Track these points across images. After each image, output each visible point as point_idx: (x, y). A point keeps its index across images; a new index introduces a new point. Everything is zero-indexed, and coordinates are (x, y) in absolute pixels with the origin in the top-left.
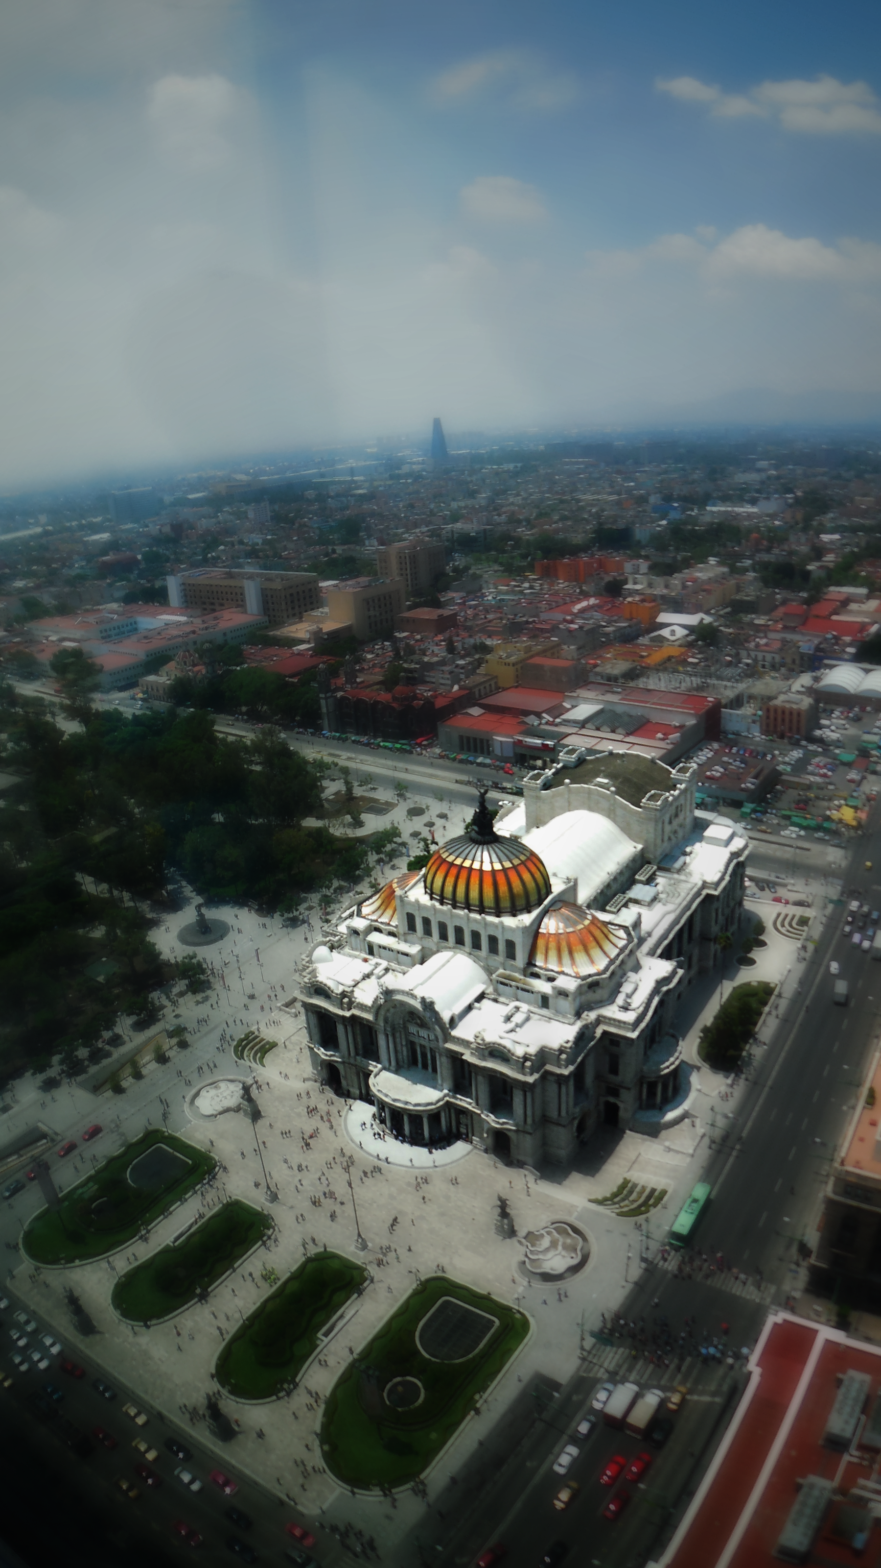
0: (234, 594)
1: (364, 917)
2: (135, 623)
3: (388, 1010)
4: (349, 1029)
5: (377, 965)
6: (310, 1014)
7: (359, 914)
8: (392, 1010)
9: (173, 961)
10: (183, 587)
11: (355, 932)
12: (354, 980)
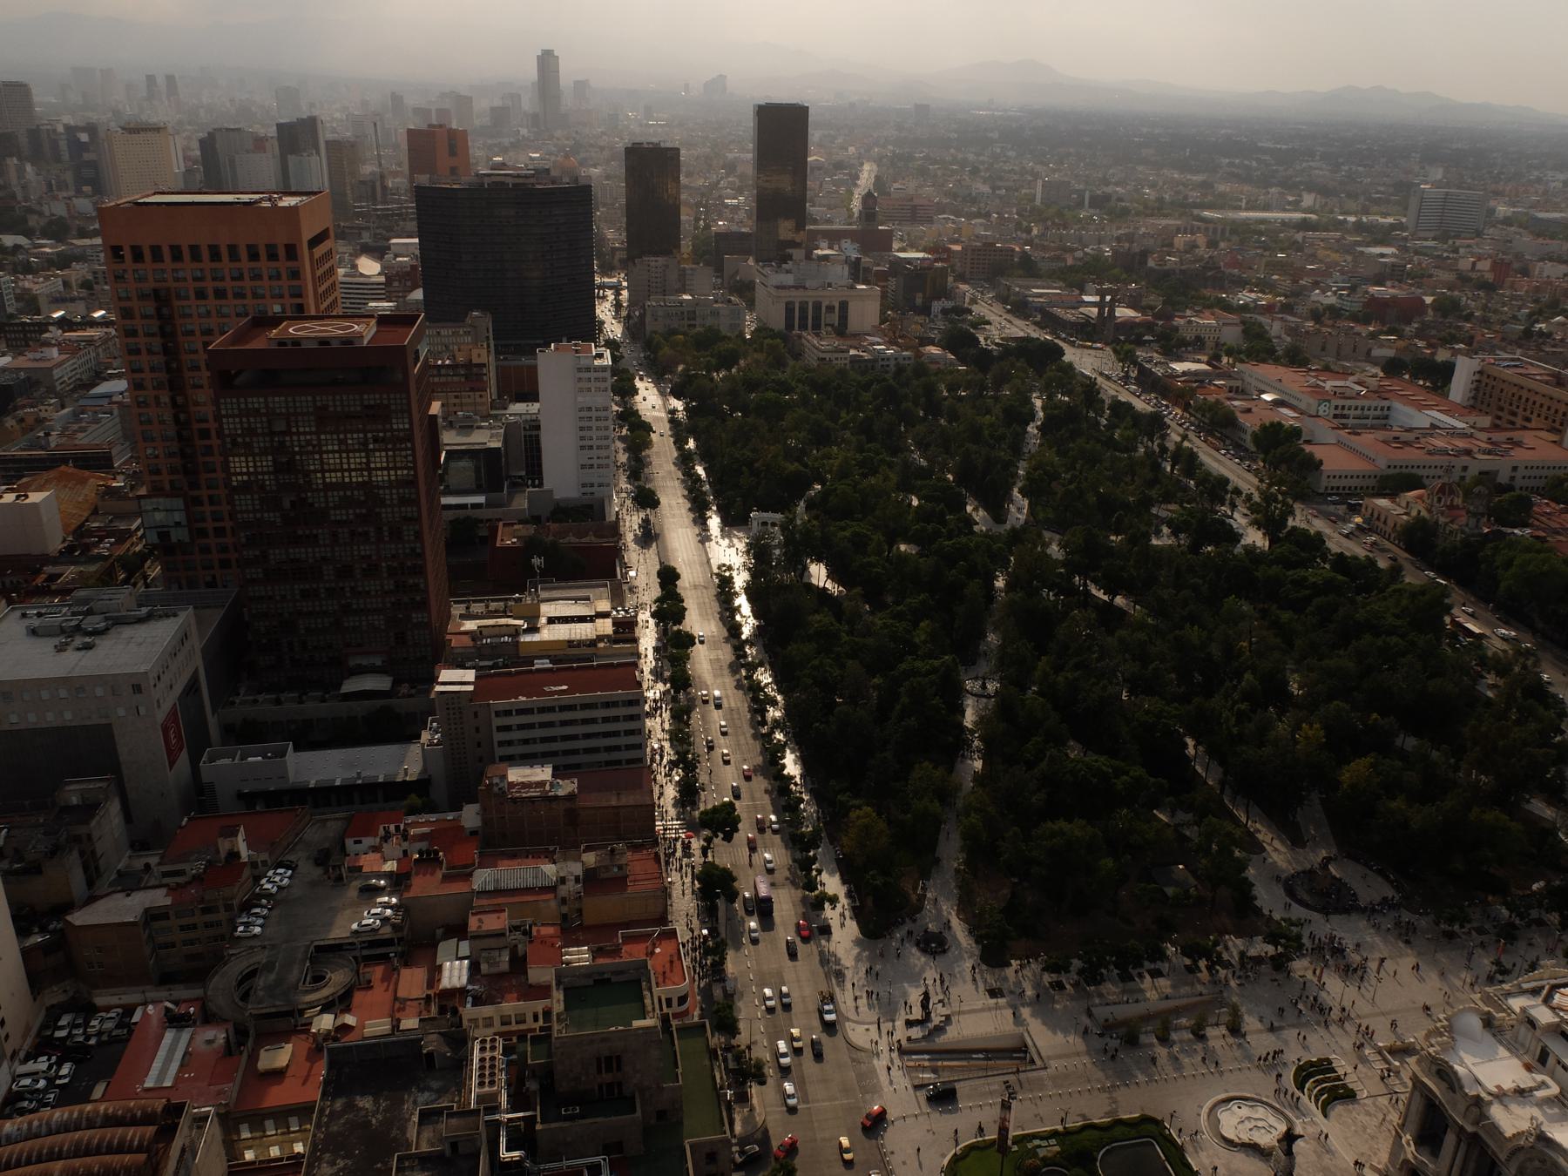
0: (1553, 411)
1: (1553, 1009)
2: (1389, 408)
3: (1531, 1160)
4: (1463, 1146)
5: (1543, 1085)
6: (1417, 1094)
7: (1547, 1001)
8: (1537, 1163)
9: (1266, 912)
10: (1477, 377)
11: (1531, 1023)
12: (1498, 1087)
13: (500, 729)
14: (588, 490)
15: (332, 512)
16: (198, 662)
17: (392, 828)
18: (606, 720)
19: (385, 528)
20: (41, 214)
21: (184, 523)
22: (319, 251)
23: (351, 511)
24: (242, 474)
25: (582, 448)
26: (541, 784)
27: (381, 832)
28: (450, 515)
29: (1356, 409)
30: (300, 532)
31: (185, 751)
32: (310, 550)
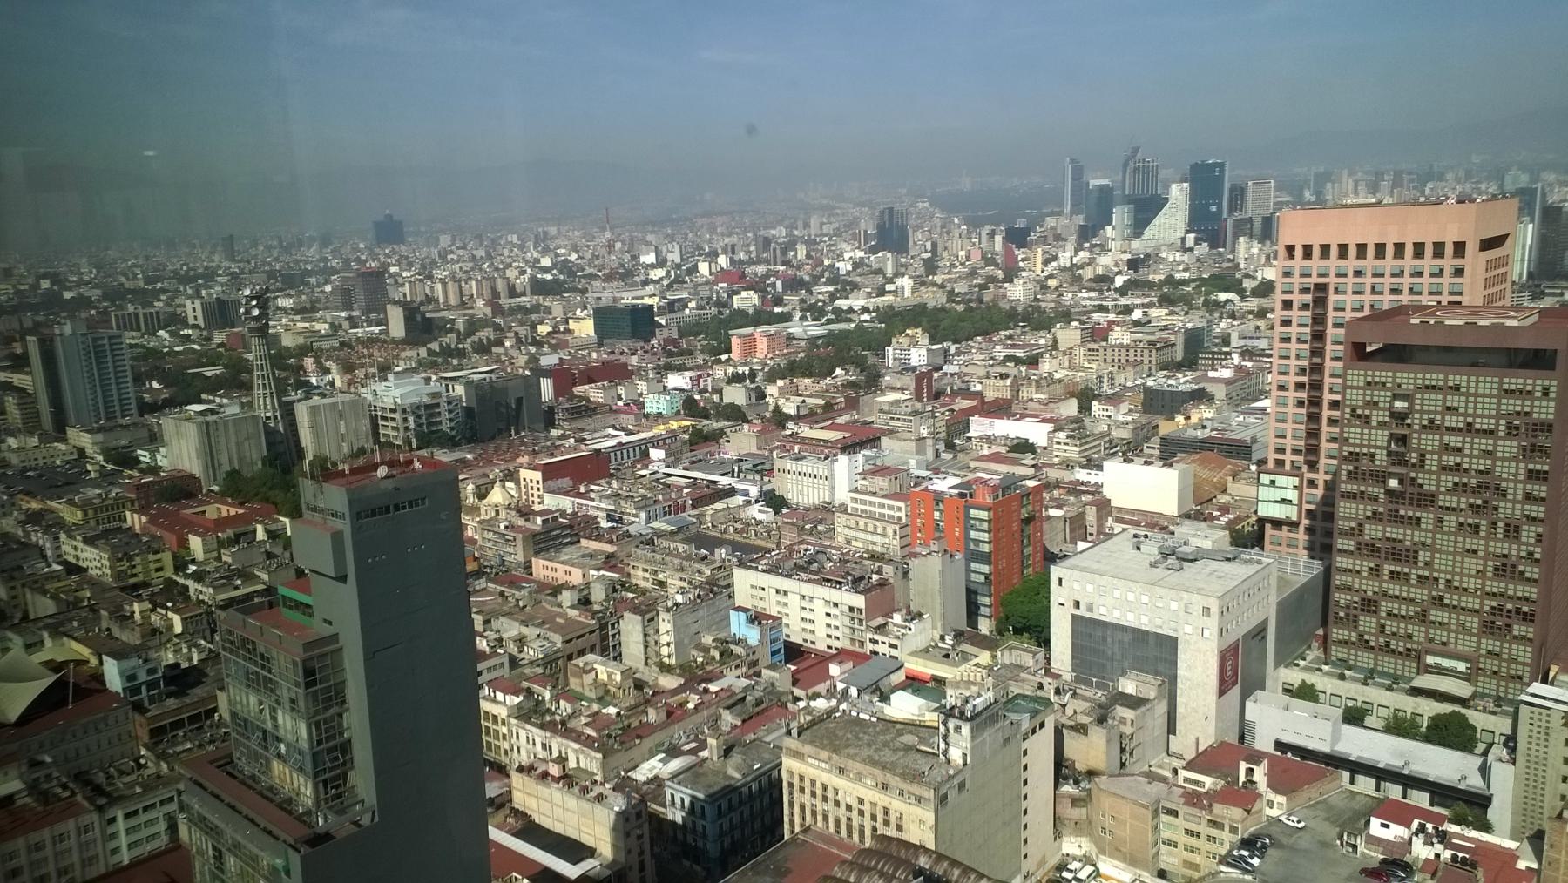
15: (1441, 497)
19: (1501, 524)
20: (1254, 278)
21: (1295, 501)
23: (1463, 500)
24: (1354, 445)
27: (1416, 824)
30: (1402, 512)
32: (1409, 532)
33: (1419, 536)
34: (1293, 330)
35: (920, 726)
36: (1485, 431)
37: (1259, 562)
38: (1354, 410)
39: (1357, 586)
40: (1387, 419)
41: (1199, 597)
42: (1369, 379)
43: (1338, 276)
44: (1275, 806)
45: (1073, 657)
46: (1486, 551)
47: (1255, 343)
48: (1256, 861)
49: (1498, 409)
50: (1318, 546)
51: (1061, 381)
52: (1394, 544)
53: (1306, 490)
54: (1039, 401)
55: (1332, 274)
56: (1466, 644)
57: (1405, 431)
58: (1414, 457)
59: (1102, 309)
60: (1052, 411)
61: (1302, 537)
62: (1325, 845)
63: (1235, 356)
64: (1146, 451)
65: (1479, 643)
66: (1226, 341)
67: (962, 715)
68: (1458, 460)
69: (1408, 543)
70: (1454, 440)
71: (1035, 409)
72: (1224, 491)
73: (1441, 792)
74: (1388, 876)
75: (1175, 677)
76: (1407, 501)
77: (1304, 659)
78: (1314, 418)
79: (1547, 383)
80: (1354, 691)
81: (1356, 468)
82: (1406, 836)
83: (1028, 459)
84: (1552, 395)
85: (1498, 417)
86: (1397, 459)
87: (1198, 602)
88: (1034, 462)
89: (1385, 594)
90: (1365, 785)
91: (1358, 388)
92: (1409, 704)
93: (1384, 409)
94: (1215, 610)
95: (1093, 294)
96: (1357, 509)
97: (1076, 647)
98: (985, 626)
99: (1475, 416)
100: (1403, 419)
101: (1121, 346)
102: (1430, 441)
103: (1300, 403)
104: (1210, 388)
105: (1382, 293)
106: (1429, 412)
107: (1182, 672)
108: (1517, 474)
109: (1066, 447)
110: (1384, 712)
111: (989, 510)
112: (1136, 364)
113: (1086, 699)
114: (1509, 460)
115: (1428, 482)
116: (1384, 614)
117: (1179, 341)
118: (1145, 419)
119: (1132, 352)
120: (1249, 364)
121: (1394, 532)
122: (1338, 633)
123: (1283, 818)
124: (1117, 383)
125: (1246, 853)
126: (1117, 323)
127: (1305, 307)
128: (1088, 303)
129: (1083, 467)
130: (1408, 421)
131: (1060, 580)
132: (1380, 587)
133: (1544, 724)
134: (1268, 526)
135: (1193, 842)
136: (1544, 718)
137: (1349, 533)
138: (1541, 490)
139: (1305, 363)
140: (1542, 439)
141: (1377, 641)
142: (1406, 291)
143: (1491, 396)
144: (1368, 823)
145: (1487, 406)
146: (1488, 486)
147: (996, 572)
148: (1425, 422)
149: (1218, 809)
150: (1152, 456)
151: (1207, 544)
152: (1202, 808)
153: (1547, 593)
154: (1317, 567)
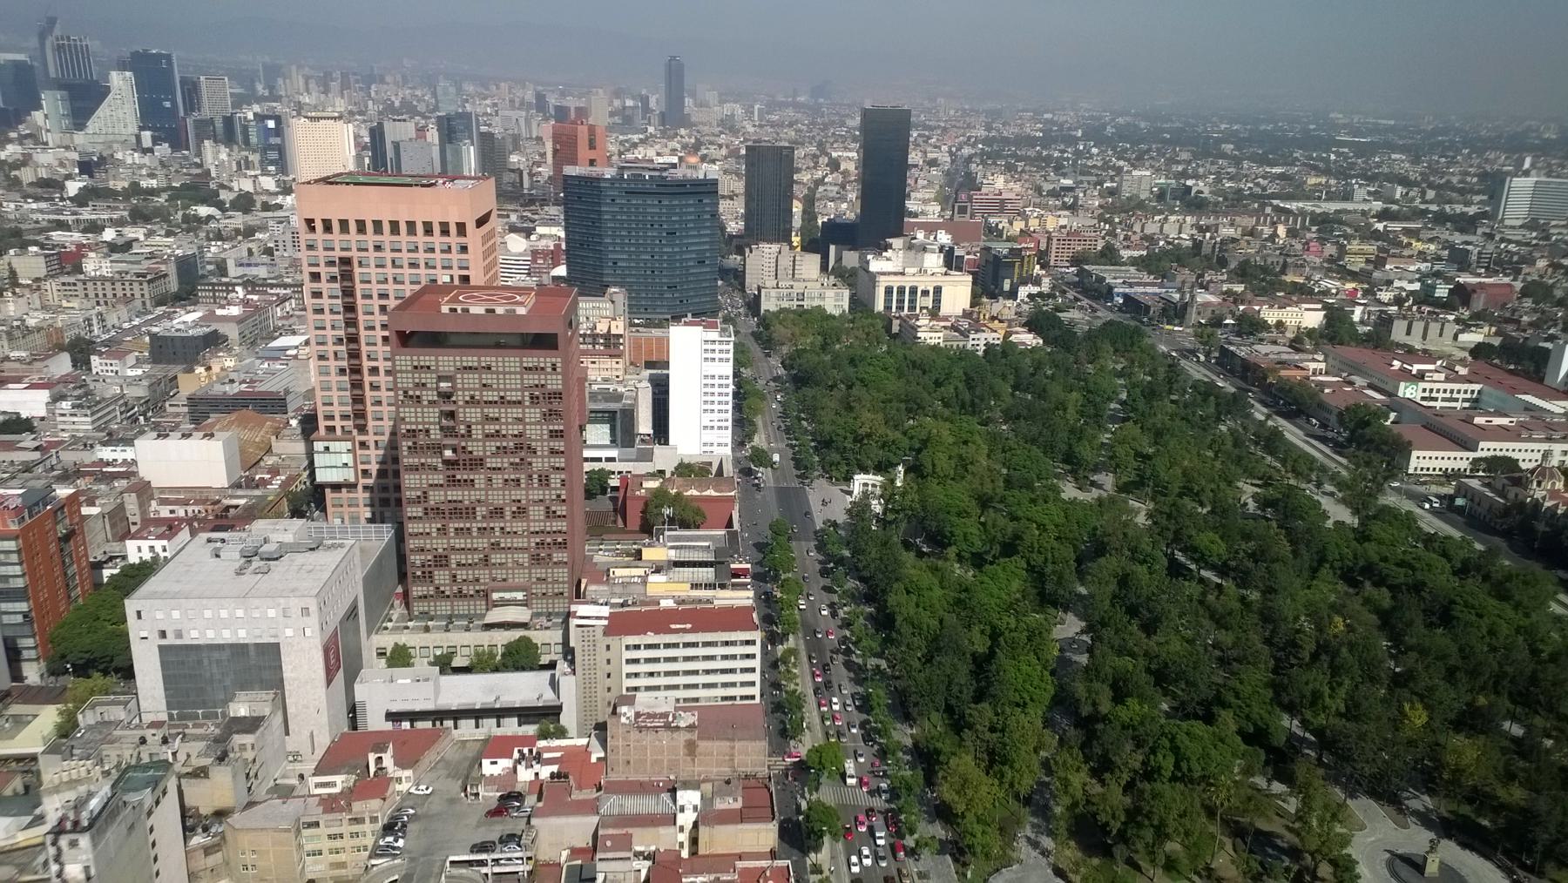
13: (628, 661)
14: (708, 448)
16: (360, 591)
17: (526, 751)
18: (725, 657)
19: (535, 476)
20: (231, 189)
21: (351, 464)
22: (486, 228)
23: (505, 460)
24: (411, 423)
25: (705, 411)
26: (665, 715)
28: (588, 467)
29: (1445, 391)
30: (458, 477)
31: (341, 670)
33: (475, 495)
34: (325, 302)
35: (9, 851)
36: (514, 402)
37: (341, 546)
38: (405, 392)
39: (428, 546)
40: (436, 398)
41: (296, 600)
42: (416, 363)
43: (359, 250)
44: (405, 782)
45: (166, 689)
46: (527, 499)
47: (253, 271)
48: (401, 843)
49: (522, 384)
50: (377, 503)
51: (39, 329)
52: (454, 505)
53: (359, 452)
54: (18, 360)
55: (354, 248)
56: (520, 577)
57: (452, 408)
58: (462, 429)
59: (62, 226)
60: (39, 371)
61: (361, 496)
62: (452, 801)
63: (239, 289)
64: (170, 410)
65: (530, 573)
66: (222, 269)
67: (76, 827)
68: (497, 427)
69: (467, 502)
70: (493, 412)
71: (16, 370)
72: (269, 451)
73: (525, 714)
74: (507, 810)
75: (282, 680)
76: (461, 467)
77: (391, 620)
78: (357, 385)
79: (554, 360)
80: (439, 640)
81: (415, 443)
82: (511, 766)
83: (27, 440)
84: (559, 370)
85: (523, 389)
86: (449, 432)
87: (295, 604)
88: (36, 444)
89: (453, 549)
90: (467, 729)
91: (407, 372)
92: (485, 639)
93: (431, 389)
94: (313, 608)
95: (43, 205)
96: (421, 479)
97: (168, 680)
98: (33, 673)
99: (505, 390)
100: (449, 397)
101: (103, 279)
102: (473, 414)
103: (342, 371)
104: (223, 329)
105: (401, 267)
106: (469, 389)
107: (288, 673)
108: (542, 435)
109: (75, 419)
110: (466, 651)
111: (16, 538)
112: (128, 300)
113: (197, 738)
114: (535, 424)
115: (476, 448)
116: (454, 566)
117: (171, 269)
118: (160, 371)
119: (118, 286)
120: (255, 298)
121: (454, 494)
122: (417, 590)
123: (413, 790)
124: (109, 326)
125: (390, 839)
126: (90, 248)
127: (333, 279)
128: (40, 217)
129: (105, 444)
130: (454, 398)
131: (139, 613)
132: (449, 543)
133: (591, 638)
134: (328, 491)
135: (338, 844)
136: (591, 634)
137: (417, 501)
138: (559, 445)
139: (341, 333)
140: (555, 405)
141: (451, 590)
142: (422, 265)
143: (515, 373)
144: (481, 764)
145: (514, 381)
146: (522, 446)
147: (38, 606)
148: (467, 398)
149: (357, 806)
150: (178, 415)
151: (288, 538)
152: (342, 810)
153: (571, 525)
154: (387, 532)
